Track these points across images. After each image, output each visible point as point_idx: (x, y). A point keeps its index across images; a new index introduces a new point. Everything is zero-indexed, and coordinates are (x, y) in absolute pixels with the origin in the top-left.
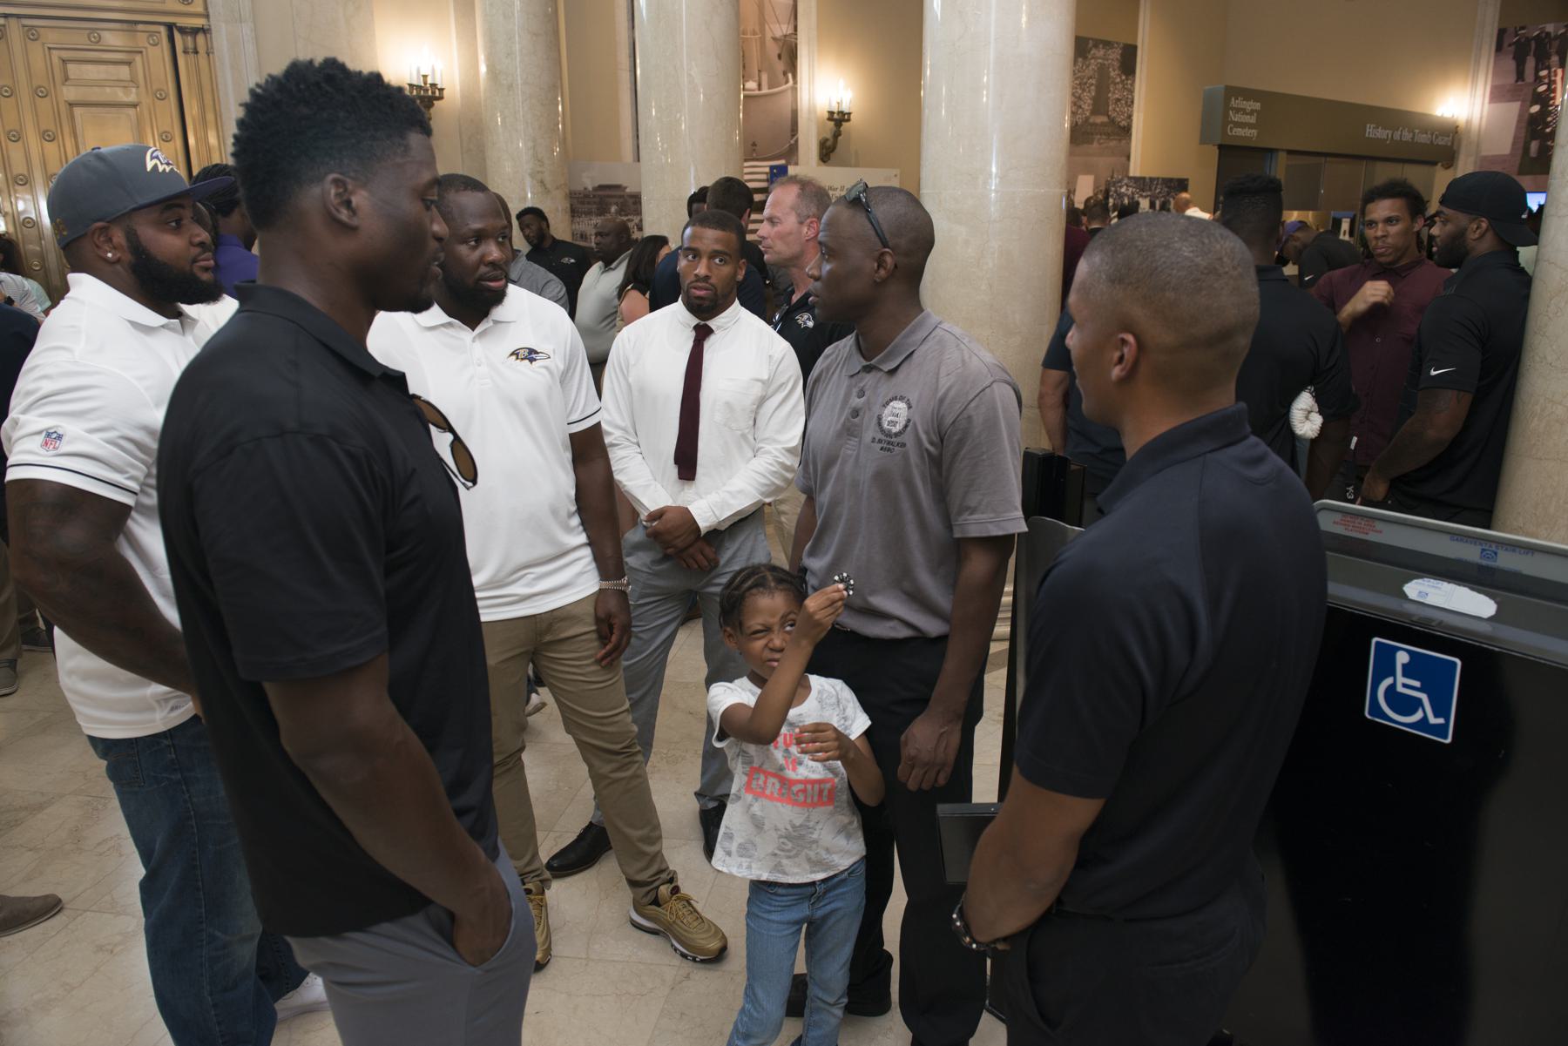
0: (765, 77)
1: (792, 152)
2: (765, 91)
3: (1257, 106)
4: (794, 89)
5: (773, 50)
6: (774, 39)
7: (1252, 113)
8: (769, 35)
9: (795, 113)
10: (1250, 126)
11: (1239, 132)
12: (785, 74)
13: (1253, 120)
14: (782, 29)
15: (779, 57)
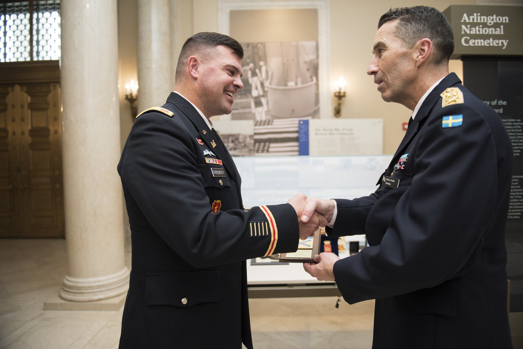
0: (299, 80)
1: (315, 114)
2: (299, 85)
3: (505, 19)
4: (317, 85)
5: (304, 67)
6: (305, 62)
7: (496, 25)
8: (301, 61)
9: (317, 95)
10: (496, 37)
11: (479, 43)
12: (311, 77)
13: (500, 31)
14: (312, 57)
15: (308, 70)
